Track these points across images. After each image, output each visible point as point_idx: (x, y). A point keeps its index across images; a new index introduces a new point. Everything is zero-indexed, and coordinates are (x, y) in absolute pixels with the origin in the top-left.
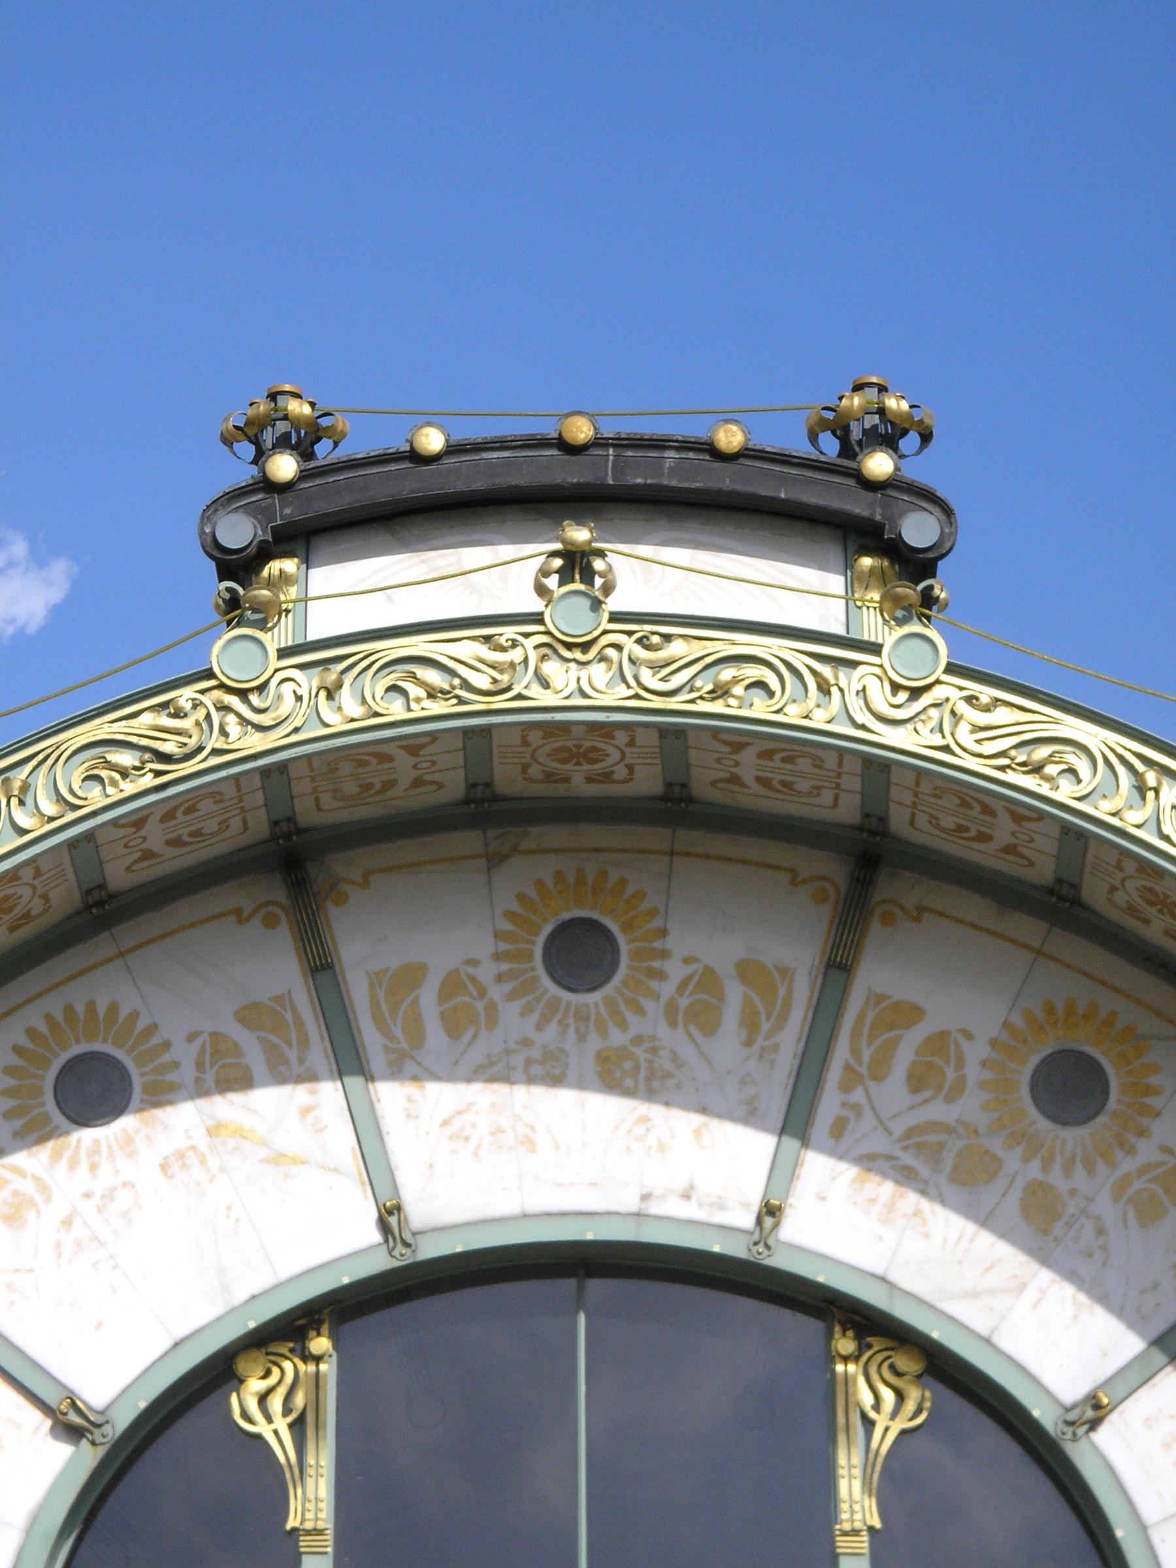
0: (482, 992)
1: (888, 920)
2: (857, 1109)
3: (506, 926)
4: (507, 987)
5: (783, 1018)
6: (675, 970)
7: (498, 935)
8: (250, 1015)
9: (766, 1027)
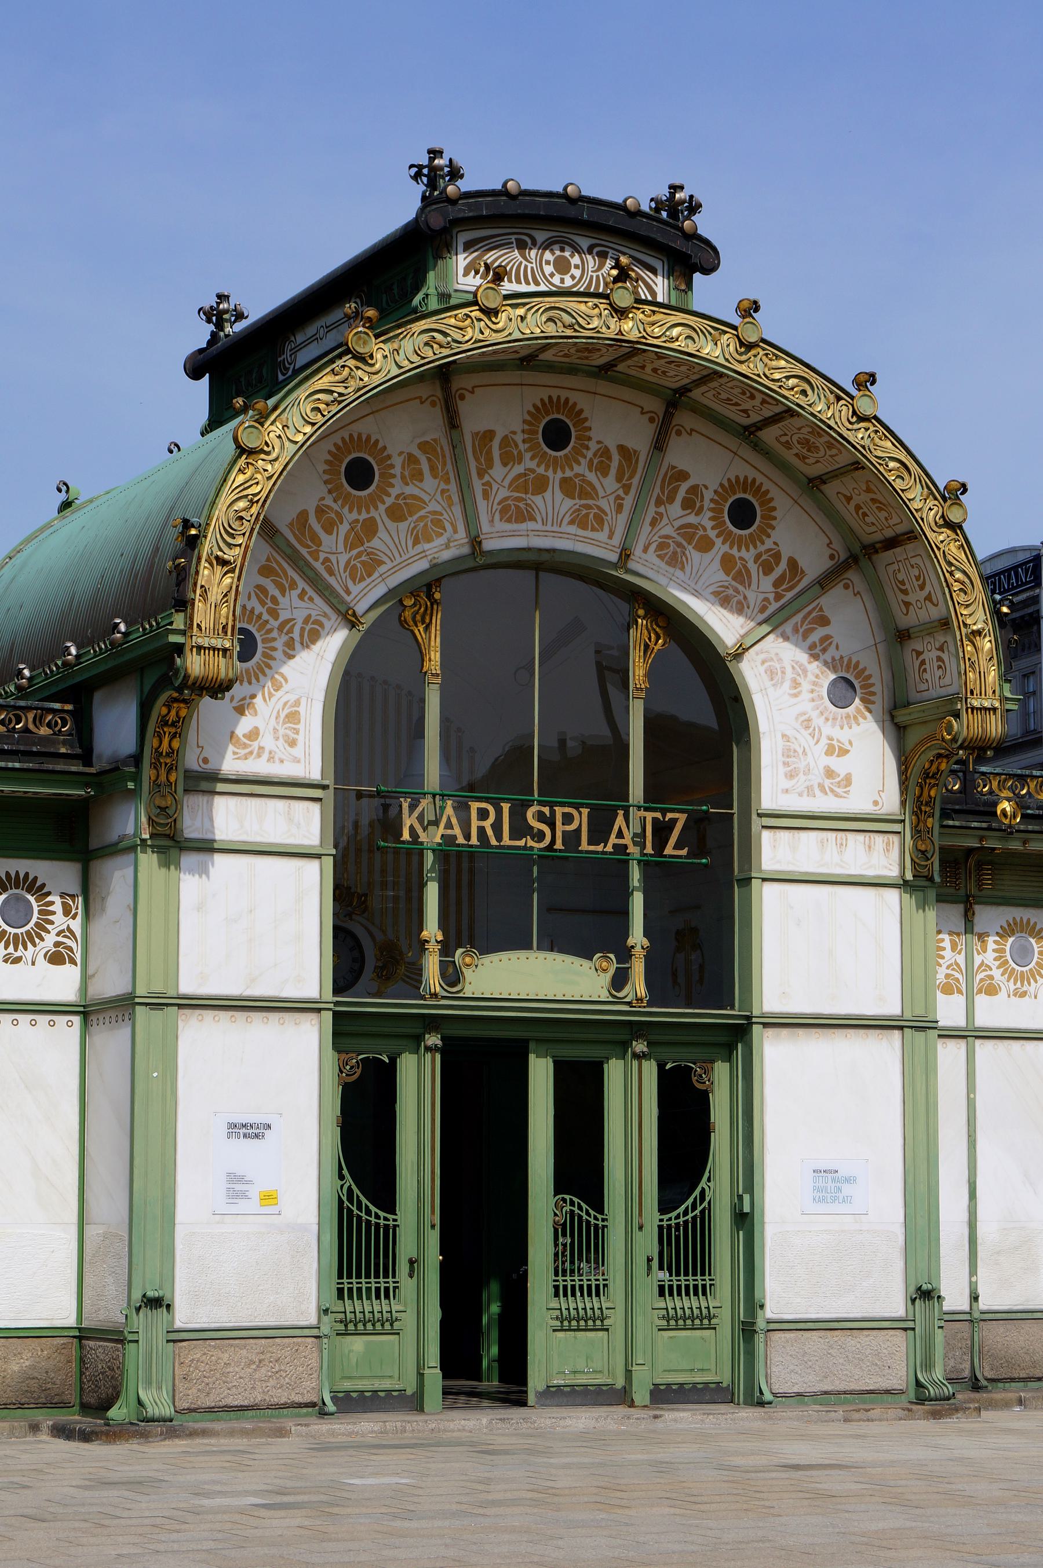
0: (516, 445)
1: (679, 433)
2: (661, 515)
3: (528, 418)
4: (527, 446)
5: (634, 472)
6: (593, 446)
7: (524, 421)
8: (424, 447)
9: (627, 476)
